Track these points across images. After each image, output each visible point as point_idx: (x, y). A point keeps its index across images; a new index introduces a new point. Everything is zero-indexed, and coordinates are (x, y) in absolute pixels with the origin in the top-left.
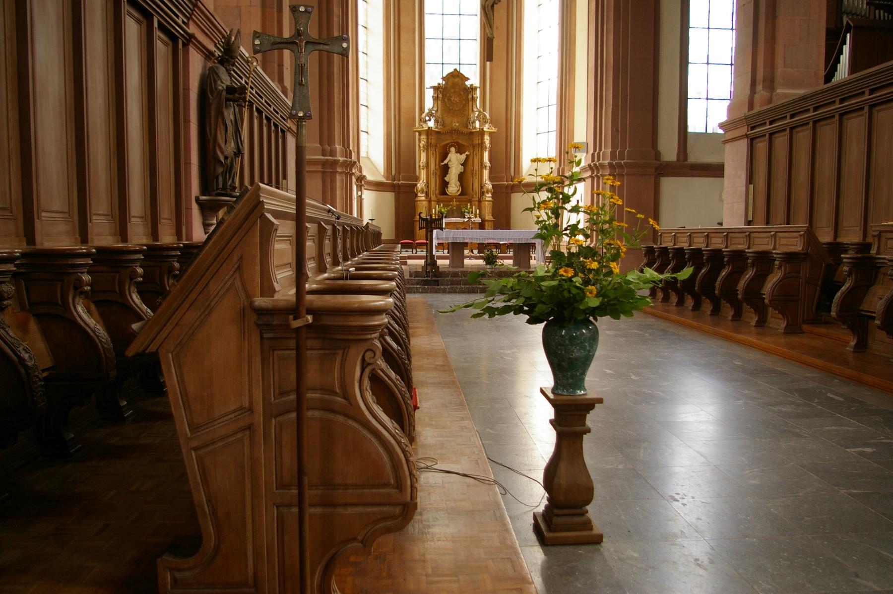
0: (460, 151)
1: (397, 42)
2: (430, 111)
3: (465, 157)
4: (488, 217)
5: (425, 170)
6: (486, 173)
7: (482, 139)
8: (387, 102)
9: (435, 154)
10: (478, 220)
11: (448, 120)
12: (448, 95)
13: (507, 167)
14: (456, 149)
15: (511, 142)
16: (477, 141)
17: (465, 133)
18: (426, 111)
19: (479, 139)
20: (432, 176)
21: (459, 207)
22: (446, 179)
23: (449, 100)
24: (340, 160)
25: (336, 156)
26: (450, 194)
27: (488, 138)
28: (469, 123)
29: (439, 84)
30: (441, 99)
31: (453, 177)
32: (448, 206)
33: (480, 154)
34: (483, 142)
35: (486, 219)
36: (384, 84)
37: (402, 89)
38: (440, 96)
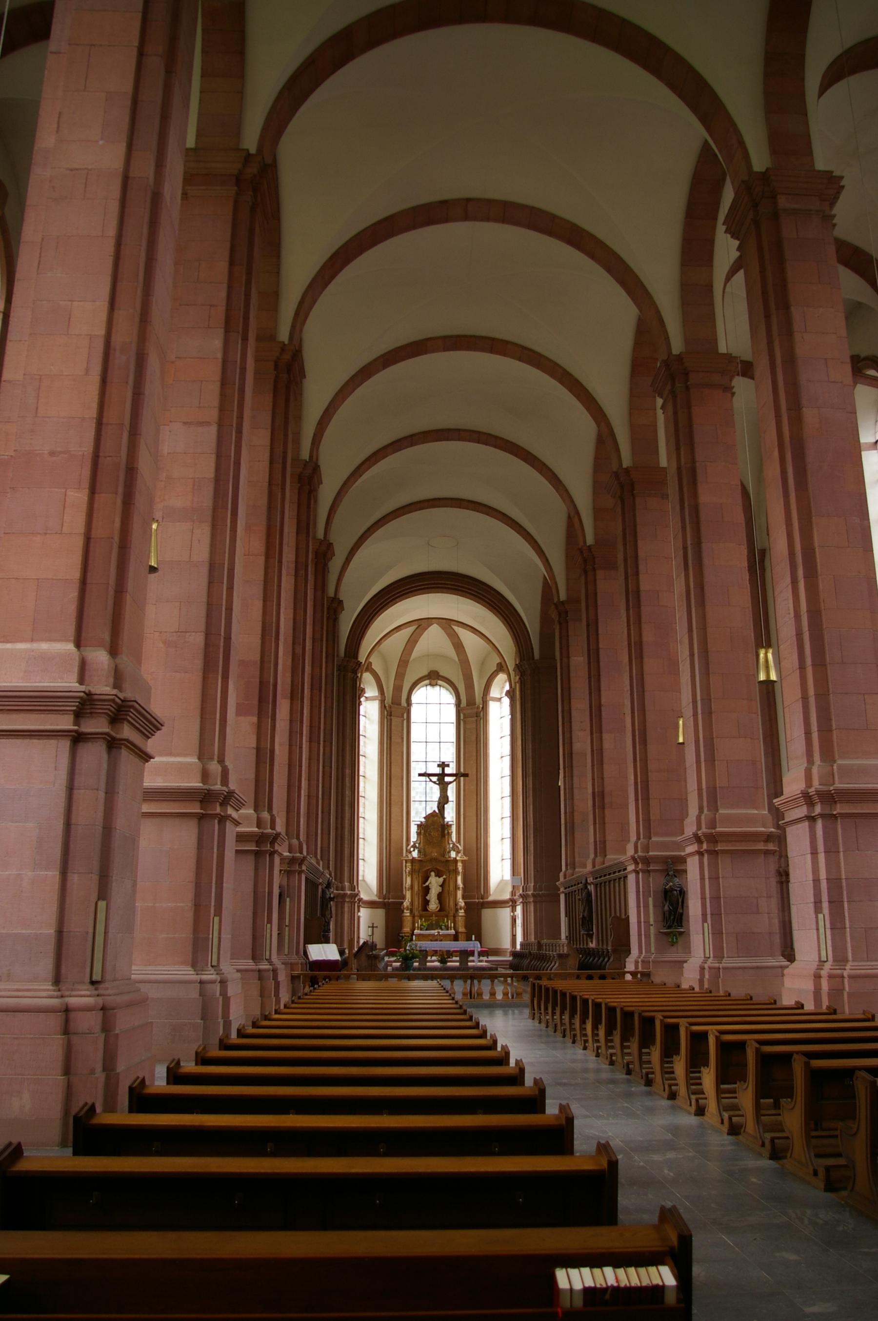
0: (439, 875)
2: (415, 843)
4: (462, 929)
5: (410, 892)
6: (460, 893)
7: (456, 866)
10: (453, 932)
12: (429, 830)
13: (478, 887)
15: (481, 866)
16: (451, 868)
18: (412, 844)
21: (437, 922)
22: (428, 898)
23: (430, 834)
27: (461, 864)
31: (433, 896)
32: (429, 920)
38: (423, 831)
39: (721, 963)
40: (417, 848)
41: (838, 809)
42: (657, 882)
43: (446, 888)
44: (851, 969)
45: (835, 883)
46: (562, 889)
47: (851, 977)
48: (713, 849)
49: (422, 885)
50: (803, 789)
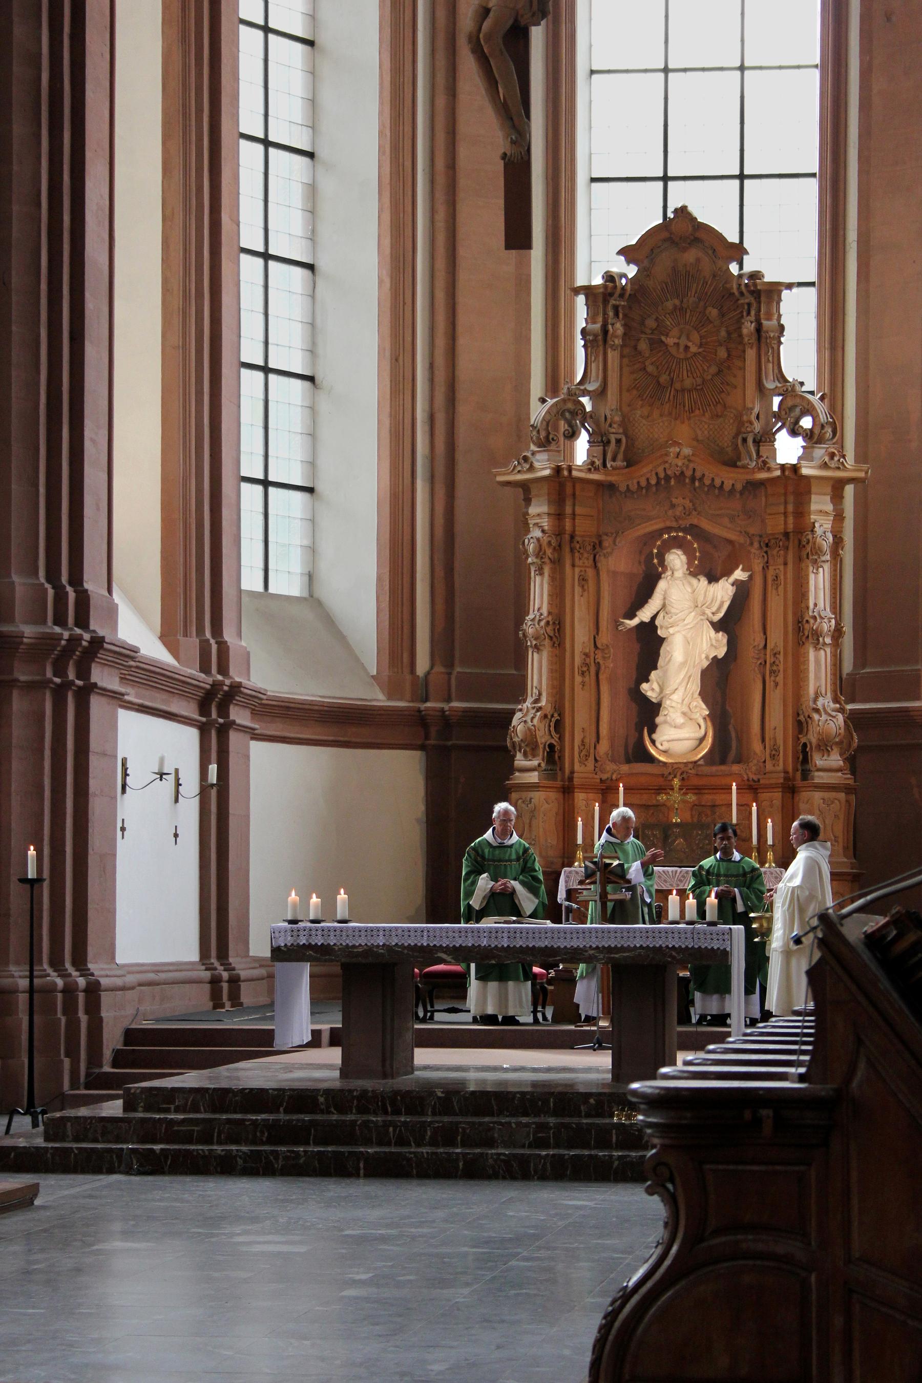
1: (441, 102)
7: (801, 512)
8: (395, 359)
9: (591, 584)
12: (651, 323)
17: (728, 486)
19: (785, 514)
20: (578, 679)
22: (650, 690)
23: (657, 344)
26: (662, 758)
28: (745, 440)
29: (609, 277)
30: (618, 342)
33: (790, 575)
36: (381, 282)
37: (464, 300)
43: (752, 636)
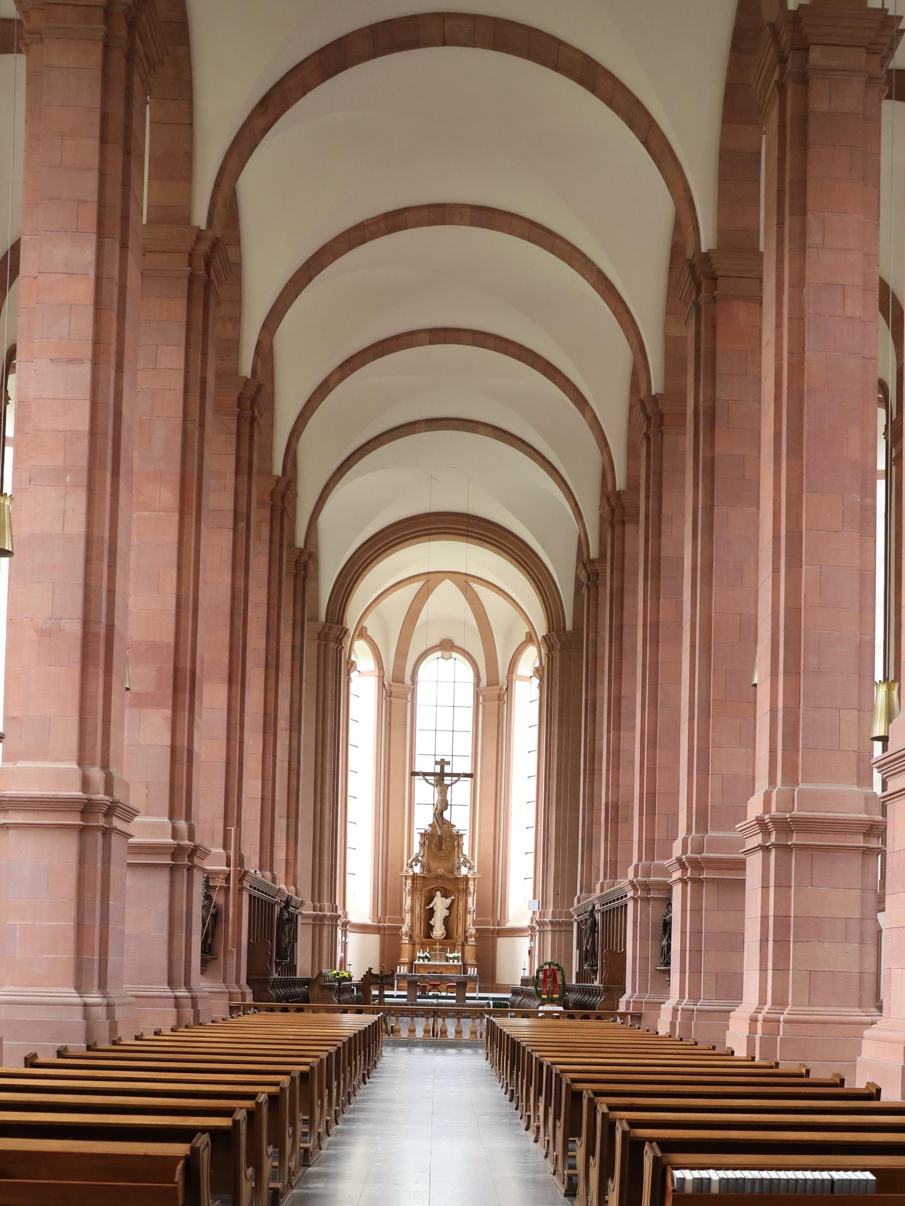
0: (445, 896)
3: (450, 901)
7: (467, 885)
11: (434, 865)
14: (441, 893)
16: (461, 887)
22: (432, 922)
24: (327, 915)
25: (324, 911)
34: (467, 888)
35: (469, 963)
38: (427, 842)
39: (696, 1005)
40: (419, 861)
41: (795, 839)
42: (654, 912)
44: (788, 1014)
45: (782, 921)
46: (575, 917)
47: (787, 1022)
48: (698, 877)
49: (424, 907)
50: (759, 815)
